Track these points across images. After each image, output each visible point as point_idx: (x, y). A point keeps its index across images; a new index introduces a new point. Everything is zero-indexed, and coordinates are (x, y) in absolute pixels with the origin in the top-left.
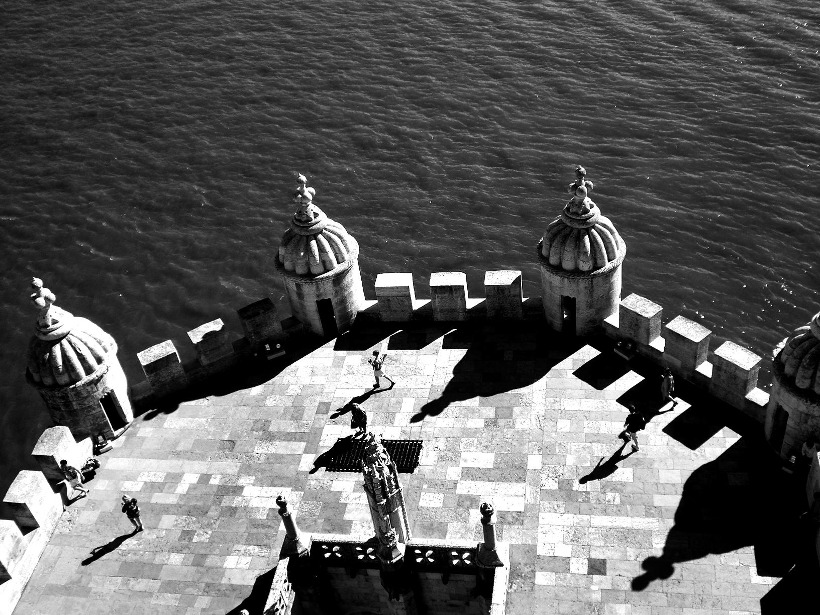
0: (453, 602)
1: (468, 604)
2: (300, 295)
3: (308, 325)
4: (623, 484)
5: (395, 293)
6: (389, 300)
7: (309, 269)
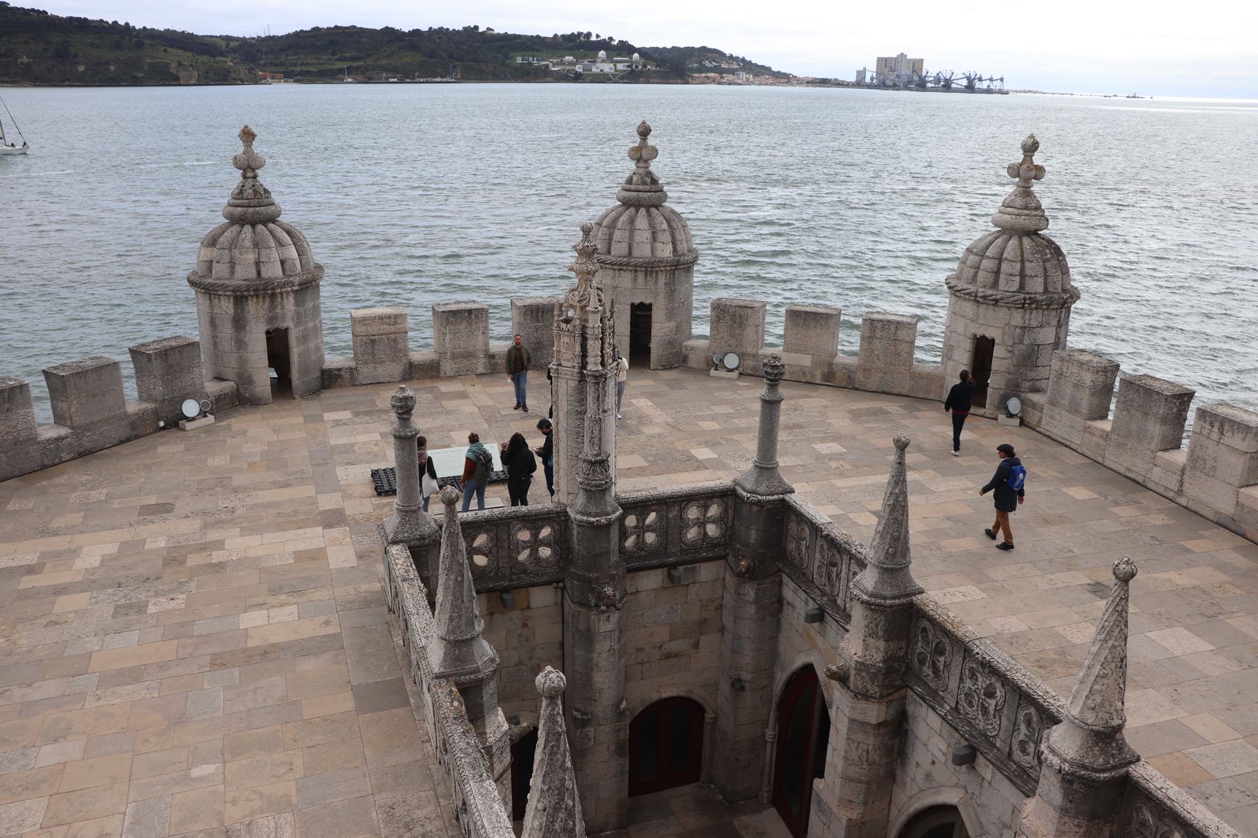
0: (673, 646)
1: (696, 646)
2: (239, 323)
3: (245, 379)
4: (841, 454)
5: (386, 328)
6: (373, 341)
7: (259, 273)
